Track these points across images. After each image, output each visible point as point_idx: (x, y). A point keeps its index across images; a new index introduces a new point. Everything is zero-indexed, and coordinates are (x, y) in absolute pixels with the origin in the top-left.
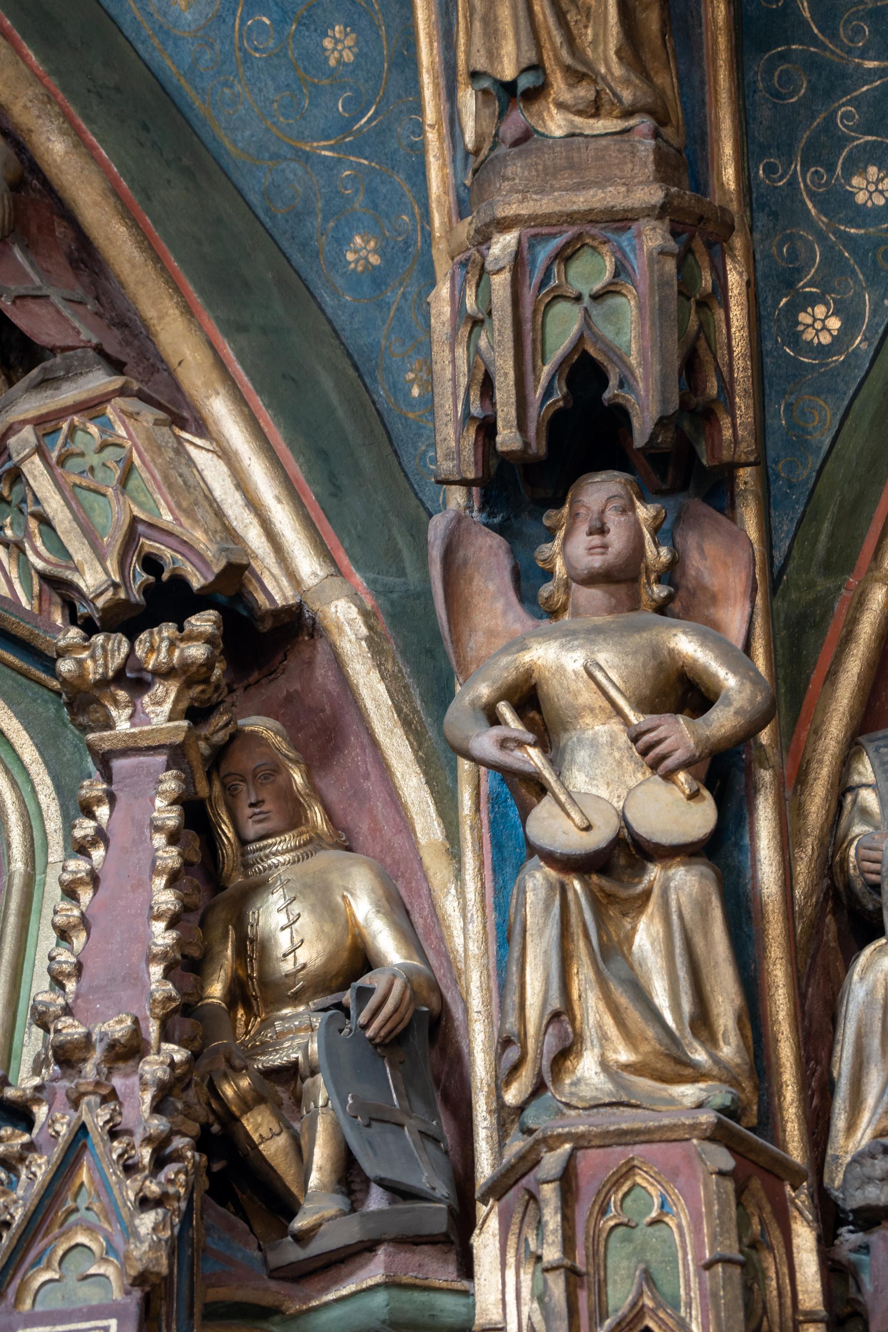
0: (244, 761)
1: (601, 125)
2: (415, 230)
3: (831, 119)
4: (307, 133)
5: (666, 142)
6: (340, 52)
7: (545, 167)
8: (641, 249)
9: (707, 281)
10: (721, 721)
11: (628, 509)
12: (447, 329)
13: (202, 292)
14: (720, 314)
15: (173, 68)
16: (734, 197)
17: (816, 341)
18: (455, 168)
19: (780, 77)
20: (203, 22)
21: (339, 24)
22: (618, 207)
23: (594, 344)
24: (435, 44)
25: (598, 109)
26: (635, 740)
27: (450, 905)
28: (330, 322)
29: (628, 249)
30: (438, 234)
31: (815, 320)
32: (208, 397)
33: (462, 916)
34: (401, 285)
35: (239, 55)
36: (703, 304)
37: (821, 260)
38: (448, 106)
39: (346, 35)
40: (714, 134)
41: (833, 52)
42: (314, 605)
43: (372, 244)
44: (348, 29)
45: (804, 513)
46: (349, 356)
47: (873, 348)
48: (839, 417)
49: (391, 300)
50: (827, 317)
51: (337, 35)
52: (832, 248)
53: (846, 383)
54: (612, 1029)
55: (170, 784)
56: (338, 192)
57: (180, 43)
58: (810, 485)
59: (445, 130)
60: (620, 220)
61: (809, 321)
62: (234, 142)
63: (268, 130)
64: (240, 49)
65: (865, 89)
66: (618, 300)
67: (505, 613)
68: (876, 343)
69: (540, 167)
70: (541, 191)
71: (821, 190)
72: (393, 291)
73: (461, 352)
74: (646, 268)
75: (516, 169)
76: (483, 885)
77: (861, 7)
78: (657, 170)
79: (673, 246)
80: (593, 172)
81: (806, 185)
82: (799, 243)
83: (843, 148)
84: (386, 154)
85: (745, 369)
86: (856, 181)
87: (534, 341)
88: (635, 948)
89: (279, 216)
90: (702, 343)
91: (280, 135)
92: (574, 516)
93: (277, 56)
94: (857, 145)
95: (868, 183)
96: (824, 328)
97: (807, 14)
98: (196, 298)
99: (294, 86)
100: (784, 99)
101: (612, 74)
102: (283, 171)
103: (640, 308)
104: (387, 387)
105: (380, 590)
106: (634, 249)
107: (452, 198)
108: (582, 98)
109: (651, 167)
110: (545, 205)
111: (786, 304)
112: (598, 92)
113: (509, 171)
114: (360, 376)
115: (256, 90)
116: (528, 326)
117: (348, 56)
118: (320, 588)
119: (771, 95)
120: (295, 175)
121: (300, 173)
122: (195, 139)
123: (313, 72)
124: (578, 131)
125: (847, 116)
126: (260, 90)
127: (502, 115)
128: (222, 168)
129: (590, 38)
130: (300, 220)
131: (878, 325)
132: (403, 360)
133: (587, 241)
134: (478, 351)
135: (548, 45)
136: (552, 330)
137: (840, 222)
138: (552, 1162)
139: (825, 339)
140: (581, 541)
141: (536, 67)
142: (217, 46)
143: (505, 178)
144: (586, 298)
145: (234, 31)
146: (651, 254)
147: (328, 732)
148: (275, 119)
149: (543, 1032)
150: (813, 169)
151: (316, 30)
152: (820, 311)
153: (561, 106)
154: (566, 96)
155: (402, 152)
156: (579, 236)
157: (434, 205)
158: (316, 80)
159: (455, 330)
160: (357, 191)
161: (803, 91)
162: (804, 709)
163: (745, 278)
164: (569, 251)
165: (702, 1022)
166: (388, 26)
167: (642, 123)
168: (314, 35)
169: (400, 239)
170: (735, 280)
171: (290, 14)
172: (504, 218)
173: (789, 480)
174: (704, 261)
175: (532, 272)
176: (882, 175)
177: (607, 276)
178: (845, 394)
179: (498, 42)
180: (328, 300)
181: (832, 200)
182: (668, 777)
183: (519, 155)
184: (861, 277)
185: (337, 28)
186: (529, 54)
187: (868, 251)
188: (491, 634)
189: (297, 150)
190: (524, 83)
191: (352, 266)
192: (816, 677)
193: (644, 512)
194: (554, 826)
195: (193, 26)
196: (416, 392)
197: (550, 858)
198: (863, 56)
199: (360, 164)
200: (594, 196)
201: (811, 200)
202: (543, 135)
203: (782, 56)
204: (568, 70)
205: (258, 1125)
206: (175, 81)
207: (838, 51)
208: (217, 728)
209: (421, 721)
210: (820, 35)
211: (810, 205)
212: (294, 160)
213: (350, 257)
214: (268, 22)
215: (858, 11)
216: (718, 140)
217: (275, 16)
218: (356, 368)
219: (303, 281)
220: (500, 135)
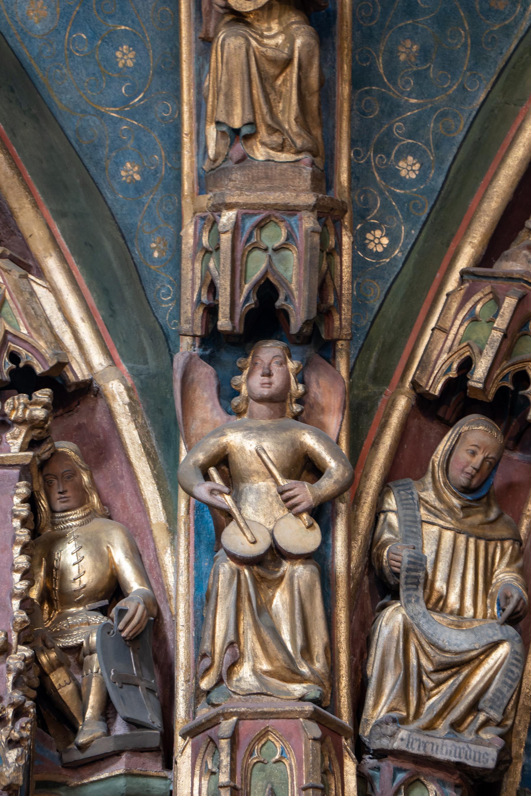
0: (58, 468)
1: (284, 157)
2: (161, 164)
3: (390, 129)
4: (103, 102)
5: (317, 167)
6: (126, 60)
7: (253, 177)
8: (302, 227)
9: (332, 242)
10: (326, 485)
11: (283, 363)
12: (191, 252)
13: (43, 193)
14: (337, 258)
15: (28, 53)
16: (346, 190)
17: (375, 250)
18: (198, 159)
19: (365, 104)
20: (47, 31)
21: (126, 45)
22: (291, 204)
23: (273, 276)
24: (192, 90)
25: (283, 148)
26: (281, 493)
27: (167, 559)
28: (110, 209)
29: (294, 226)
30: (186, 194)
31: (375, 238)
32: (46, 257)
33: (175, 567)
34: (151, 193)
35: (67, 52)
36: (330, 254)
37: (380, 206)
38: (196, 125)
39: (130, 51)
41: (394, 93)
42: (100, 382)
43: (136, 168)
44: (131, 49)
45: (363, 345)
46: (120, 230)
47: (404, 256)
48: (384, 293)
49: (145, 201)
50: (381, 237)
51: (125, 51)
52: (386, 199)
53: (389, 274)
54: (259, 652)
55: (23, 490)
56: (119, 137)
57: (33, 40)
58: (367, 330)
59: (194, 137)
60: (292, 210)
61: (372, 238)
62: (60, 100)
63: (81, 97)
64: (68, 49)
65: (409, 114)
66: (287, 252)
67: (212, 410)
68: (406, 254)
69: (250, 176)
71: (383, 167)
72: (146, 196)
73: (198, 265)
74: (304, 238)
75: (237, 176)
76: (189, 555)
77: (410, 70)
78: (312, 184)
79: (318, 227)
80: (278, 181)
81: (375, 164)
82: (369, 195)
83: (395, 145)
84: (147, 120)
85: (348, 289)
86: (402, 164)
87: (241, 271)
88: (273, 606)
89: (84, 145)
90: (328, 276)
91: (87, 100)
92: (254, 364)
93: (89, 56)
94: (403, 144)
95: (408, 165)
96: (380, 243)
97: (381, 71)
98: (40, 197)
99: (98, 75)
100: (367, 116)
101: (292, 130)
102: (88, 120)
103: (299, 259)
104: (139, 249)
105: (136, 374)
106: (297, 227)
107: (195, 174)
108: (275, 142)
109: (309, 182)
110: (252, 198)
111: (360, 228)
112: (284, 139)
113: (233, 177)
114: (126, 242)
115: (75, 74)
116: (238, 263)
117: (130, 63)
118: (103, 373)
119: (360, 113)
120: (95, 123)
121: (98, 123)
122: (39, 96)
123: (109, 69)
124: (272, 159)
125: (399, 128)
126: (78, 74)
127: (231, 145)
128: (52, 114)
129: (281, 108)
130: (96, 149)
131: (408, 244)
132: (150, 236)
133: (273, 219)
134: (208, 269)
135: (259, 112)
137: (392, 185)
138: (226, 726)
139: (380, 249)
140: (257, 379)
141: (252, 124)
142: (55, 46)
143: (231, 180)
144: (270, 250)
145: (64, 39)
146: (306, 231)
147: (102, 449)
148: (85, 91)
149: (223, 652)
150: (379, 156)
151: (112, 46)
152: (378, 233)
153: (263, 144)
155: (157, 121)
156: (269, 217)
157: (185, 178)
158: (110, 74)
160: (129, 138)
161: (377, 112)
162: (359, 460)
163: (352, 240)
164: (263, 223)
165: (307, 651)
166: (154, 51)
168: (111, 48)
169: (152, 168)
170: (346, 240)
171: (98, 35)
172: (230, 203)
173: (356, 326)
174: (332, 231)
175: (242, 233)
176: (415, 162)
177: (283, 239)
178: (388, 280)
179: (232, 107)
180: (109, 196)
182: (298, 515)
183: (240, 168)
184: (401, 216)
185: (125, 47)
186: (249, 117)
188: (204, 421)
189: (97, 111)
190: (245, 131)
191: (124, 179)
192: (367, 443)
193: (292, 365)
194: (235, 539)
195: (41, 33)
196: (156, 255)
197: (233, 557)
198: (409, 96)
199: (133, 124)
200: (278, 196)
201: (378, 173)
202: (252, 158)
203: (367, 92)
204: (268, 127)
205: (59, 678)
206: (28, 61)
208: (44, 451)
209: (155, 453)
210: (388, 83)
213: (123, 173)
214: (85, 37)
215: (408, 71)
216: (340, 158)
217: (89, 35)
218: (124, 238)
219: (96, 184)
220: (230, 155)
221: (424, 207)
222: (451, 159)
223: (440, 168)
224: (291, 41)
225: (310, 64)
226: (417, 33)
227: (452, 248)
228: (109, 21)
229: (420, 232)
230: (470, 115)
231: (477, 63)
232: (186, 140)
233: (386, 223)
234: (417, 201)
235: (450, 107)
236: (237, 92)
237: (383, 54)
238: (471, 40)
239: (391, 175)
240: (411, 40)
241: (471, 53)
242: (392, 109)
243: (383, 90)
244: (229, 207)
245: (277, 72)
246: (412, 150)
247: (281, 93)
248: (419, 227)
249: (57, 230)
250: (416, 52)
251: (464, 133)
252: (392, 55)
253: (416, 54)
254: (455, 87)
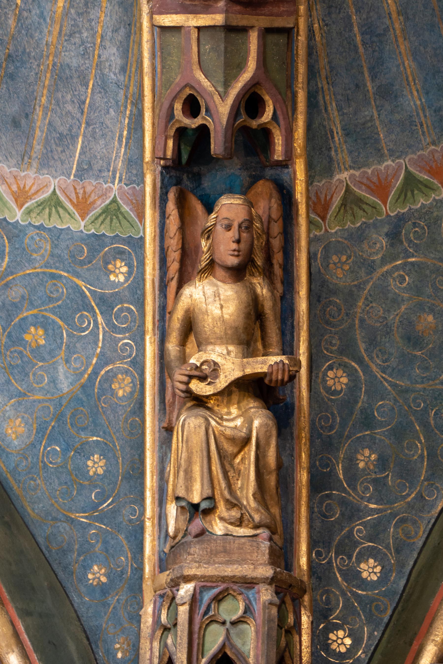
2: (127, 565)
3: (351, 532)
4: (73, 508)
5: (275, 543)
6: (96, 468)
7: (211, 551)
8: (259, 600)
9: (291, 620)
12: (149, 631)
13: (9, 592)
14: (297, 638)
15: (4, 468)
16: (306, 573)
17: (338, 650)
18: (159, 542)
19: (326, 507)
20: (23, 446)
21: (97, 454)
22: (249, 576)
23: (231, 649)
24: (155, 477)
25: (241, 522)
28: (76, 611)
29: (252, 599)
30: (147, 576)
31: (338, 638)
32: (8, 653)
34: (117, 594)
35: (41, 464)
36: (288, 632)
37: (342, 606)
38: (158, 509)
39: (100, 460)
40: (297, 539)
41: (354, 498)
43: (103, 571)
44: (102, 457)
46: (85, 632)
47: (368, 658)
49: (111, 602)
50: (344, 637)
51: (96, 460)
52: (349, 600)
56: (87, 541)
57: (10, 456)
59: (156, 521)
60: (249, 583)
61: (335, 638)
62: (33, 510)
63: (52, 505)
64: (42, 462)
65: (369, 518)
66: (245, 626)
68: (369, 655)
69: (209, 550)
70: (208, 563)
71: (344, 568)
72: (112, 598)
73: (156, 644)
74: (261, 611)
77: (369, 477)
78: (270, 558)
79: (276, 600)
80: (236, 555)
81: (337, 565)
82: (332, 595)
83: (357, 547)
84: (115, 524)
86: (363, 566)
87: (198, 644)
89: (54, 551)
90: (287, 654)
91: (58, 508)
93: (62, 467)
94: (364, 547)
95: (369, 567)
96: (342, 643)
97: (341, 477)
99: (69, 483)
100: (328, 518)
101: (250, 506)
102: (58, 527)
103: (257, 632)
104: (103, 651)
106: (255, 599)
107: (156, 557)
108: (233, 516)
109: (267, 556)
110: (210, 570)
111: (323, 627)
112: (242, 514)
113: (192, 550)
114: (90, 644)
115: (48, 484)
116: (196, 636)
117: (100, 471)
119: (321, 515)
120: (65, 530)
121: (68, 529)
122: (12, 506)
123: (80, 477)
124: (230, 533)
125: (359, 531)
126: (51, 484)
127: (190, 520)
128: (25, 523)
129: (239, 485)
130: (65, 554)
131: (371, 645)
132: (114, 637)
133: (231, 592)
134: (166, 645)
135: (218, 487)
136: (208, 639)
137: (353, 586)
139: (343, 649)
141: (211, 498)
142: (30, 459)
143: (189, 554)
144: (228, 624)
145: (40, 452)
146: (264, 603)
148: (57, 500)
150: (341, 557)
151: (84, 456)
152: (341, 633)
153: (222, 519)
154: (225, 514)
155: (124, 523)
156: (227, 589)
157: (146, 561)
158: (82, 482)
159: (154, 632)
160: (98, 542)
161: (337, 515)
163: (311, 619)
164: (221, 597)
166: (123, 458)
167: (264, 533)
168: (83, 458)
169: (119, 569)
170: (305, 619)
171: (71, 447)
172: (188, 576)
174: (290, 608)
175: (200, 606)
176: (376, 564)
177: (240, 612)
179: (191, 483)
180: (76, 599)
181: (350, 574)
183: (198, 542)
184: (363, 617)
185: (96, 456)
186: (208, 491)
187: (367, 604)
189: (67, 517)
190: (204, 505)
191: (91, 581)
195: (18, 448)
196: (120, 655)
198: (368, 501)
199: (101, 527)
200: (236, 569)
201: (339, 573)
202: (211, 533)
203: (328, 496)
204: (227, 501)
206: (4, 475)
207: (356, 497)
210: (348, 488)
211: (338, 575)
212: (65, 522)
213: (90, 576)
214: (59, 449)
215: (367, 478)
216: (299, 542)
217: (63, 447)
218: (88, 639)
219: (63, 588)
220: (189, 530)
221: (386, 609)
222: (412, 563)
223: (401, 571)
224: (251, 423)
225: (268, 444)
226: (375, 443)
227: (415, 647)
228: (82, 433)
229: (383, 634)
230: (429, 522)
231: (434, 474)
232: (148, 524)
233: (348, 623)
234: (380, 603)
235: (409, 513)
236: (197, 469)
237: (343, 461)
238: (427, 452)
239: (353, 576)
240: (369, 449)
241: (427, 464)
242: (353, 513)
243: (343, 495)
244: (187, 579)
245: (235, 450)
246: (372, 553)
247: (240, 471)
248: (382, 628)
249: (21, 627)
250: (374, 460)
251: (424, 539)
252: (351, 463)
253: (375, 463)
254: (413, 495)
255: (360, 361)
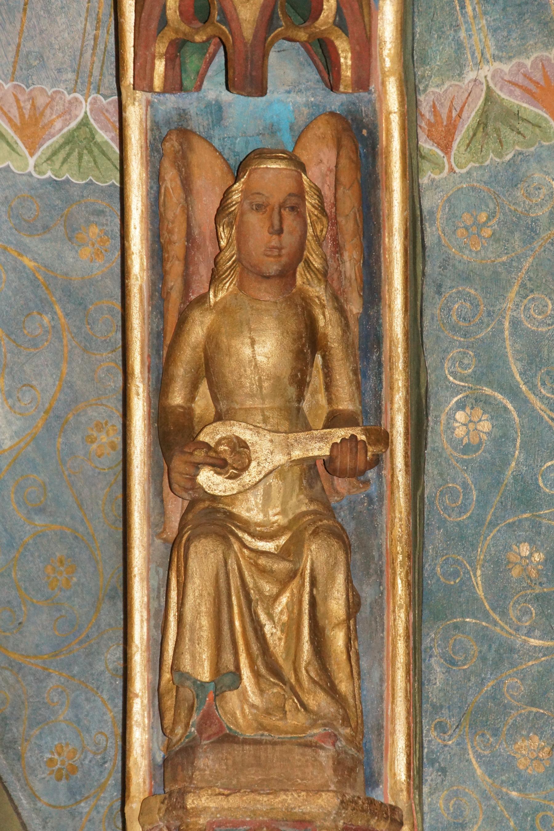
3: (497, 688)
7: (234, 763)
16: (404, 787)
19: (454, 646)
40: (390, 727)
41: (502, 629)
69: (230, 762)
77: (528, 592)
84: (92, 674)
97: (480, 592)
121: (11, 681)
198: (529, 634)
203: (456, 627)
207: (507, 627)
212: (7, 669)
215: (526, 595)
216: (393, 733)
225: (331, 578)
226: (539, 534)
237: (483, 566)
240: (530, 544)
243: (484, 624)
245: (275, 591)
250: (538, 563)
253: (540, 567)
255: (513, 393)
